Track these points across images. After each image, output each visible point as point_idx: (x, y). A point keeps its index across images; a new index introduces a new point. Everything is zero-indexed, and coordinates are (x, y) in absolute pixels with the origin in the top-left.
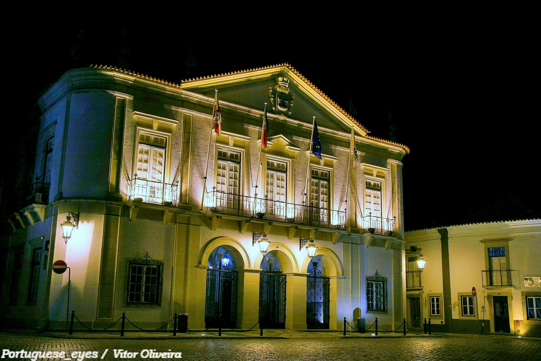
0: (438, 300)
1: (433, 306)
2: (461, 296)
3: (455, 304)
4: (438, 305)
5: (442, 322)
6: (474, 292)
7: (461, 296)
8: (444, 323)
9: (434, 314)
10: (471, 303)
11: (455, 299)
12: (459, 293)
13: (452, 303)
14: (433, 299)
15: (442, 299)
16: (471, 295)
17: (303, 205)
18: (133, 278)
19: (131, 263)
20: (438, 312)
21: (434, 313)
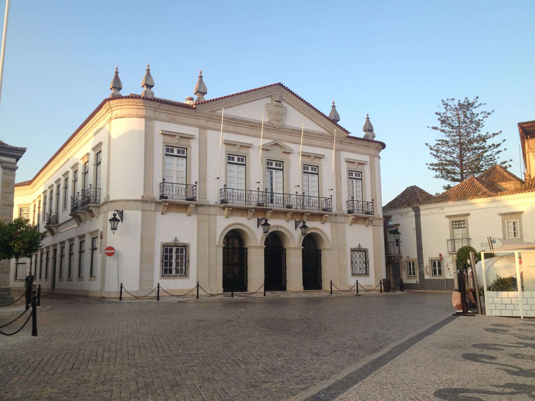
0: (413, 264)
1: (410, 269)
2: (432, 261)
3: (426, 267)
4: (414, 268)
5: (417, 282)
6: (441, 257)
7: (432, 261)
8: (418, 282)
9: (411, 275)
10: (439, 265)
11: (426, 262)
12: (429, 258)
13: (424, 266)
14: (410, 264)
15: (416, 263)
16: (439, 259)
17: (297, 195)
18: (166, 256)
19: (164, 246)
20: (414, 274)
21: (410, 274)
